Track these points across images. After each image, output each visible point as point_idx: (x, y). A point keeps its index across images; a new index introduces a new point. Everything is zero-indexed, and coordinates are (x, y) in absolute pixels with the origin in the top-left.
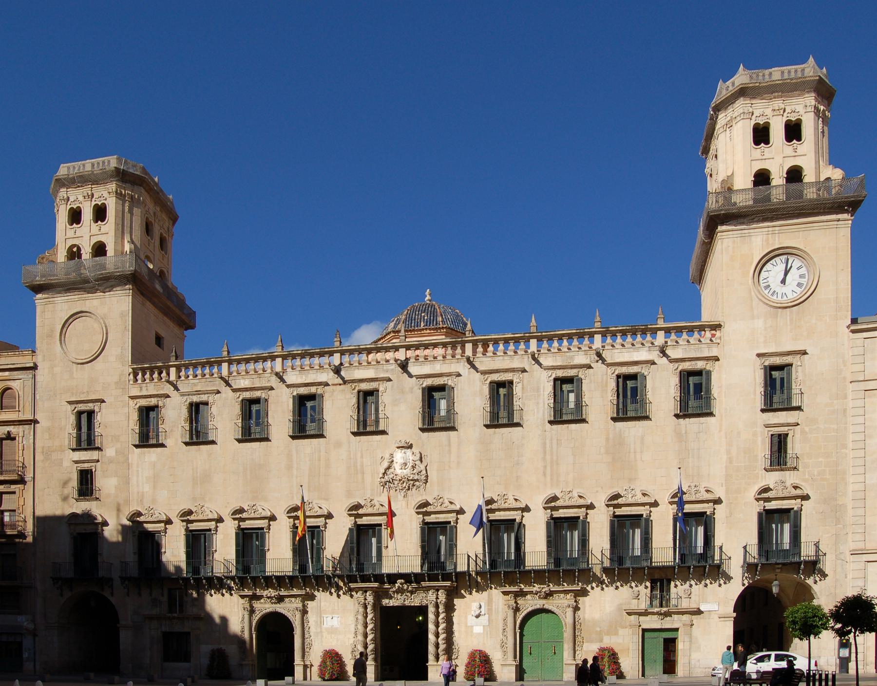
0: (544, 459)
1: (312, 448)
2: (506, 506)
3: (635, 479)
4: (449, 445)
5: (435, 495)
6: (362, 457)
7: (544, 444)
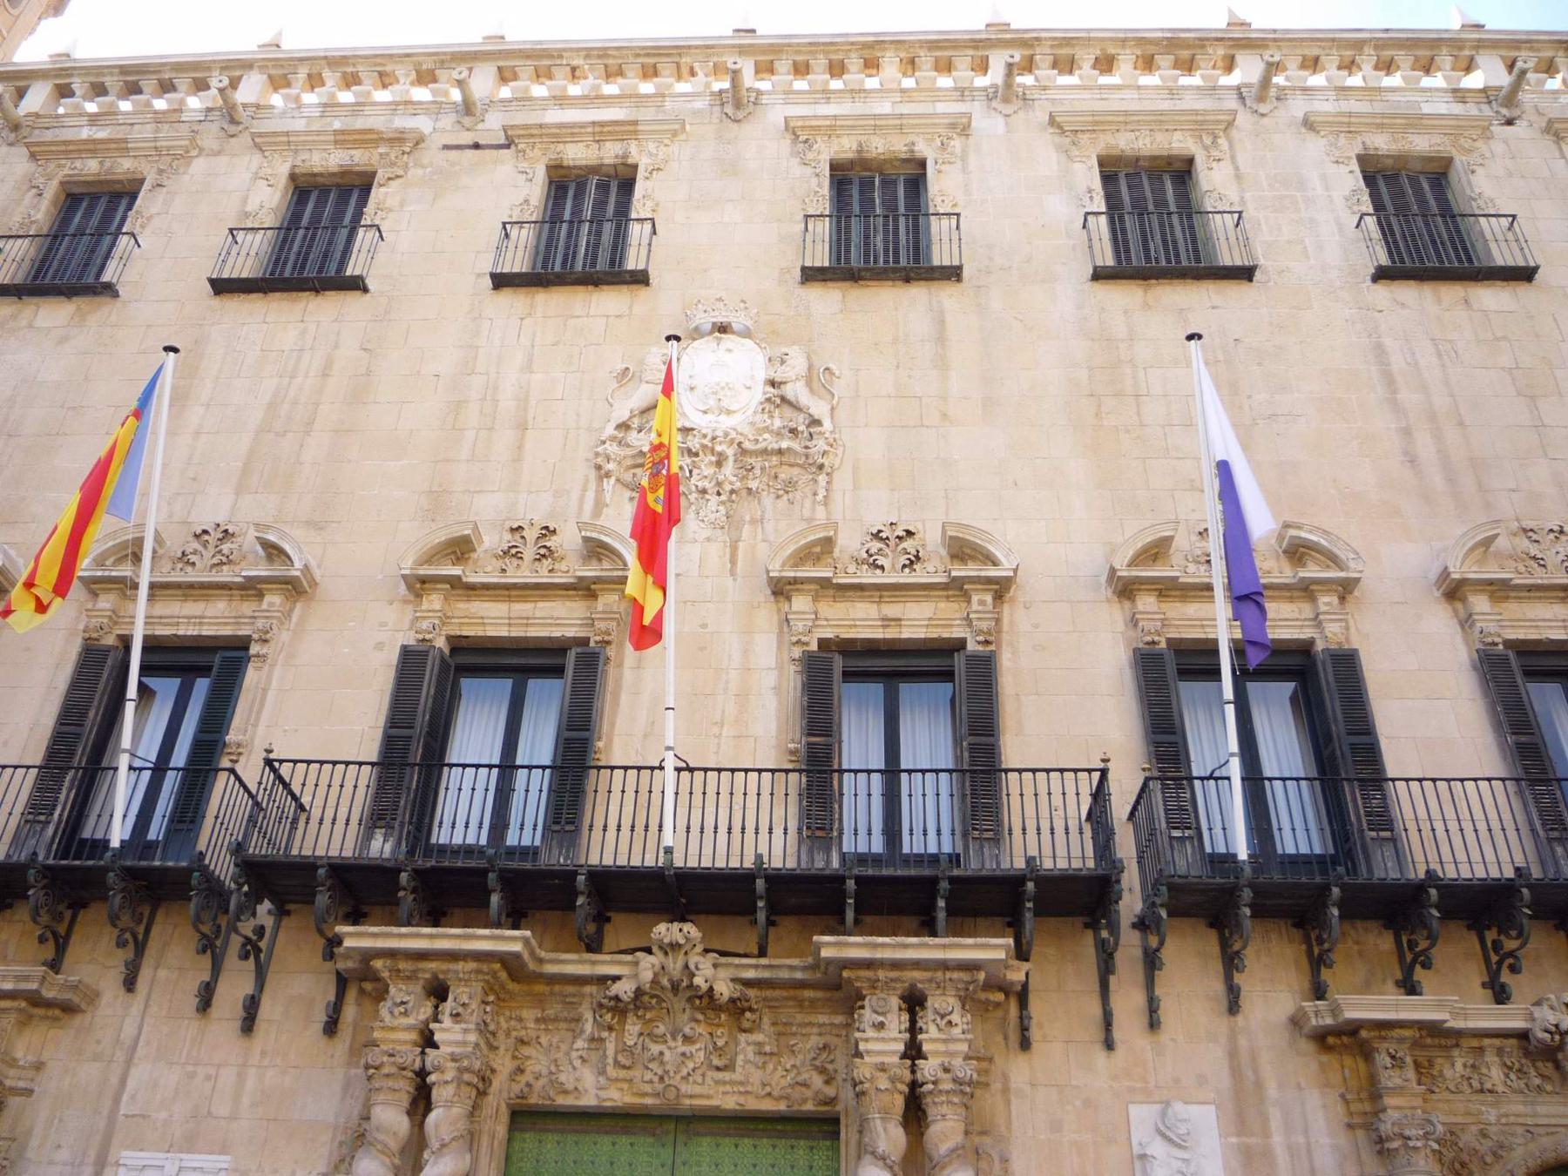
4: (941, 338)
6: (528, 367)
7: (1380, 351)
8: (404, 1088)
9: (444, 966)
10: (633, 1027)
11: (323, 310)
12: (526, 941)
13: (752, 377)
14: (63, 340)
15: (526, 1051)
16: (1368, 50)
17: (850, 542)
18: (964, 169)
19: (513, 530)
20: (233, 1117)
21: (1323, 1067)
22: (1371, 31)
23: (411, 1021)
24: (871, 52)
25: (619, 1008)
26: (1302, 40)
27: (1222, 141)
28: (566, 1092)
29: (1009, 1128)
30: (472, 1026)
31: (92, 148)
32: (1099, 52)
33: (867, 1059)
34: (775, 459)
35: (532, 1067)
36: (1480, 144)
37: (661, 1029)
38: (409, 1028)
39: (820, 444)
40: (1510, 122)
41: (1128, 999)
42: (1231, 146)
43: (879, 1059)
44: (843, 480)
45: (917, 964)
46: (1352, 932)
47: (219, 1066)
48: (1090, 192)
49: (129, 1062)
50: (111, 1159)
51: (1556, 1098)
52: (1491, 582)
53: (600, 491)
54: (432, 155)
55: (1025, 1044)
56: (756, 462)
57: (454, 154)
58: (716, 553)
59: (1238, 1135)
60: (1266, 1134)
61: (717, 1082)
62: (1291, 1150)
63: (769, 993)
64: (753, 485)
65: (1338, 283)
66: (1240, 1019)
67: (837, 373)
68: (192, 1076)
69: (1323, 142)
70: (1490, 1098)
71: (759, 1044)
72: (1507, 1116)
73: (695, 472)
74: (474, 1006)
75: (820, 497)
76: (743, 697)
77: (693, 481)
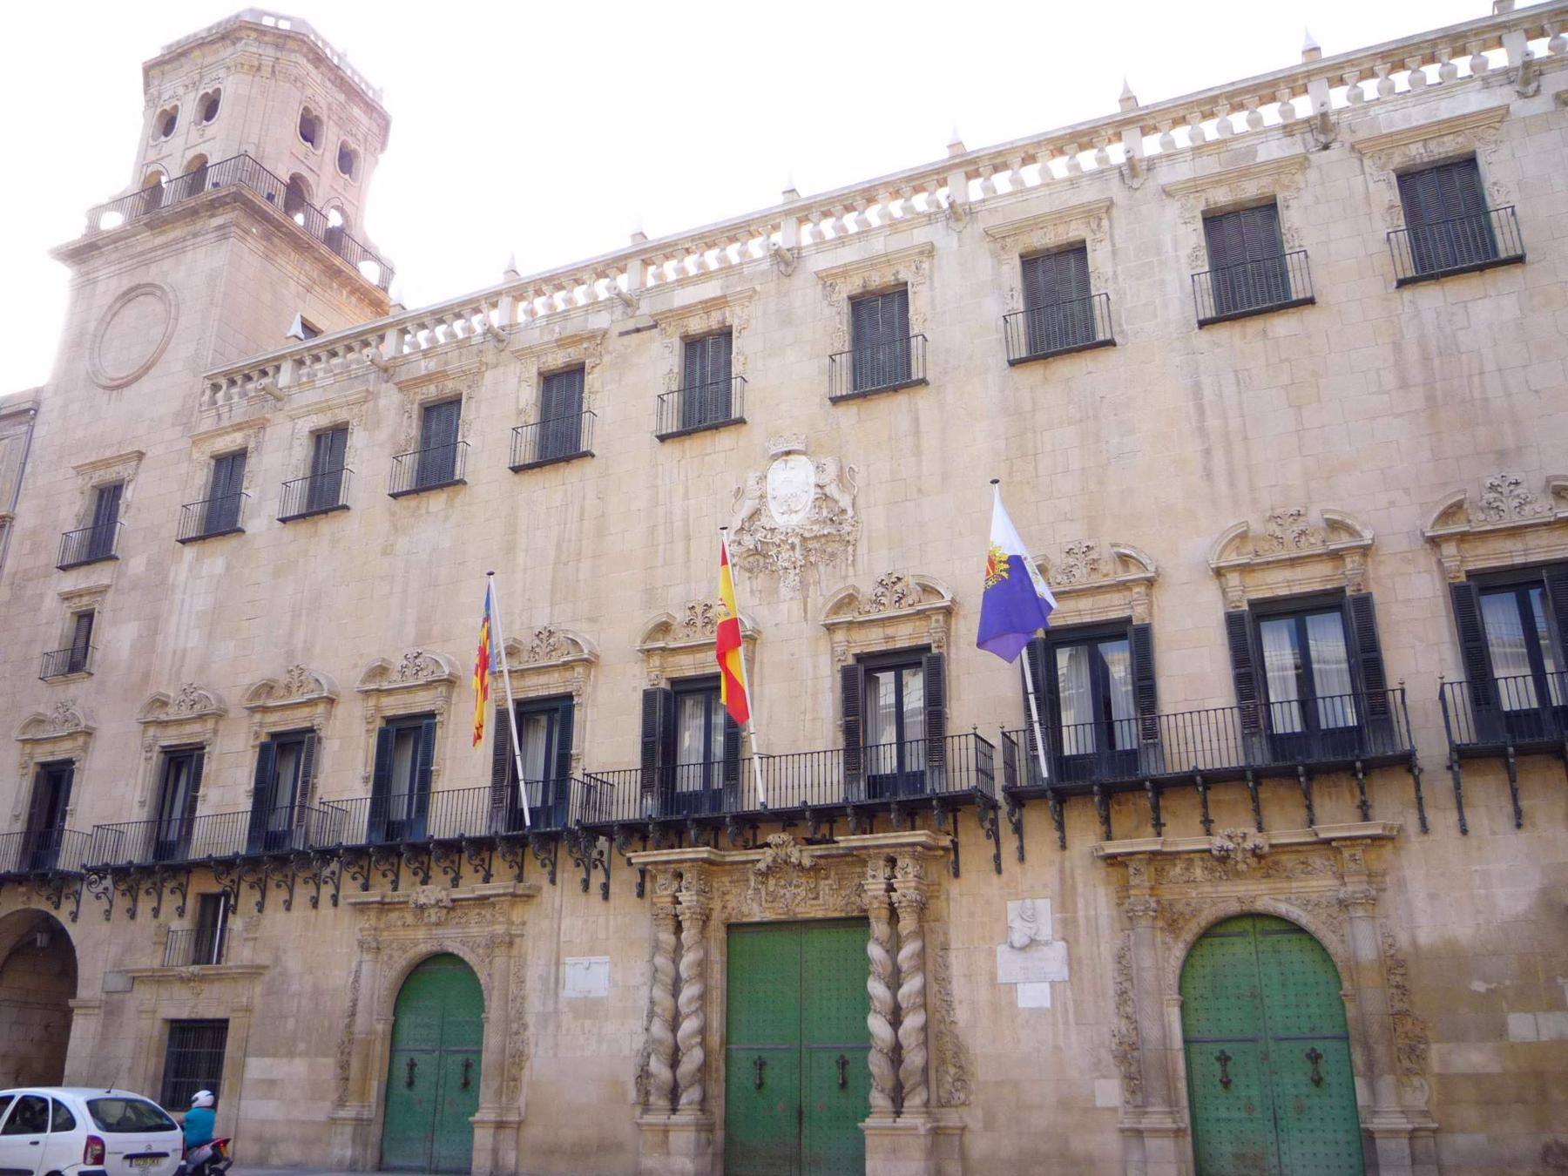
0: (1202, 430)
1: (566, 491)
2: (1097, 580)
3: (1519, 449)
4: (917, 433)
5: (881, 570)
6: (686, 496)
7: (1197, 389)
8: (670, 924)
9: (678, 865)
10: (772, 882)
11: (572, 474)
12: (709, 852)
13: (808, 484)
14: (446, 518)
15: (727, 897)
16: (1223, 101)
17: (867, 589)
18: (932, 288)
19: (690, 609)
20: (607, 939)
21: (1108, 874)
22: (1220, 87)
23: (669, 892)
24: (868, 194)
25: (765, 874)
26: (1168, 108)
27: (1105, 223)
28: (747, 916)
29: (949, 917)
30: (693, 892)
31: (430, 378)
32: (1023, 155)
33: (869, 893)
34: (823, 540)
35: (730, 905)
36: (1298, 177)
37: (783, 882)
38: (668, 896)
39: (846, 528)
40: (1326, 147)
41: (1009, 845)
42: (1111, 227)
43: (875, 893)
44: (862, 548)
45: (888, 846)
46: (1131, 797)
47: (598, 916)
48: (1012, 290)
49: (560, 918)
50: (562, 961)
51: (1229, 882)
52: (1239, 565)
54: (615, 343)
55: (957, 874)
56: (812, 545)
57: (627, 338)
58: (796, 607)
59: (1061, 912)
60: (1075, 911)
61: (812, 906)
62: (1087, 918)
63: (830, 860)
64: (813, 559)
65: (1175, 335)
66: (1067, 853)
67: (856, 470)
68: (587, 921)
69: (1178, 204)
70: (1193, 885)
71: (831, 885)
72: (1202, 893)
73: (780, 556)
74: (694, 882)
75: (849, 562)
76: (815, 695)
77: (779, 563)
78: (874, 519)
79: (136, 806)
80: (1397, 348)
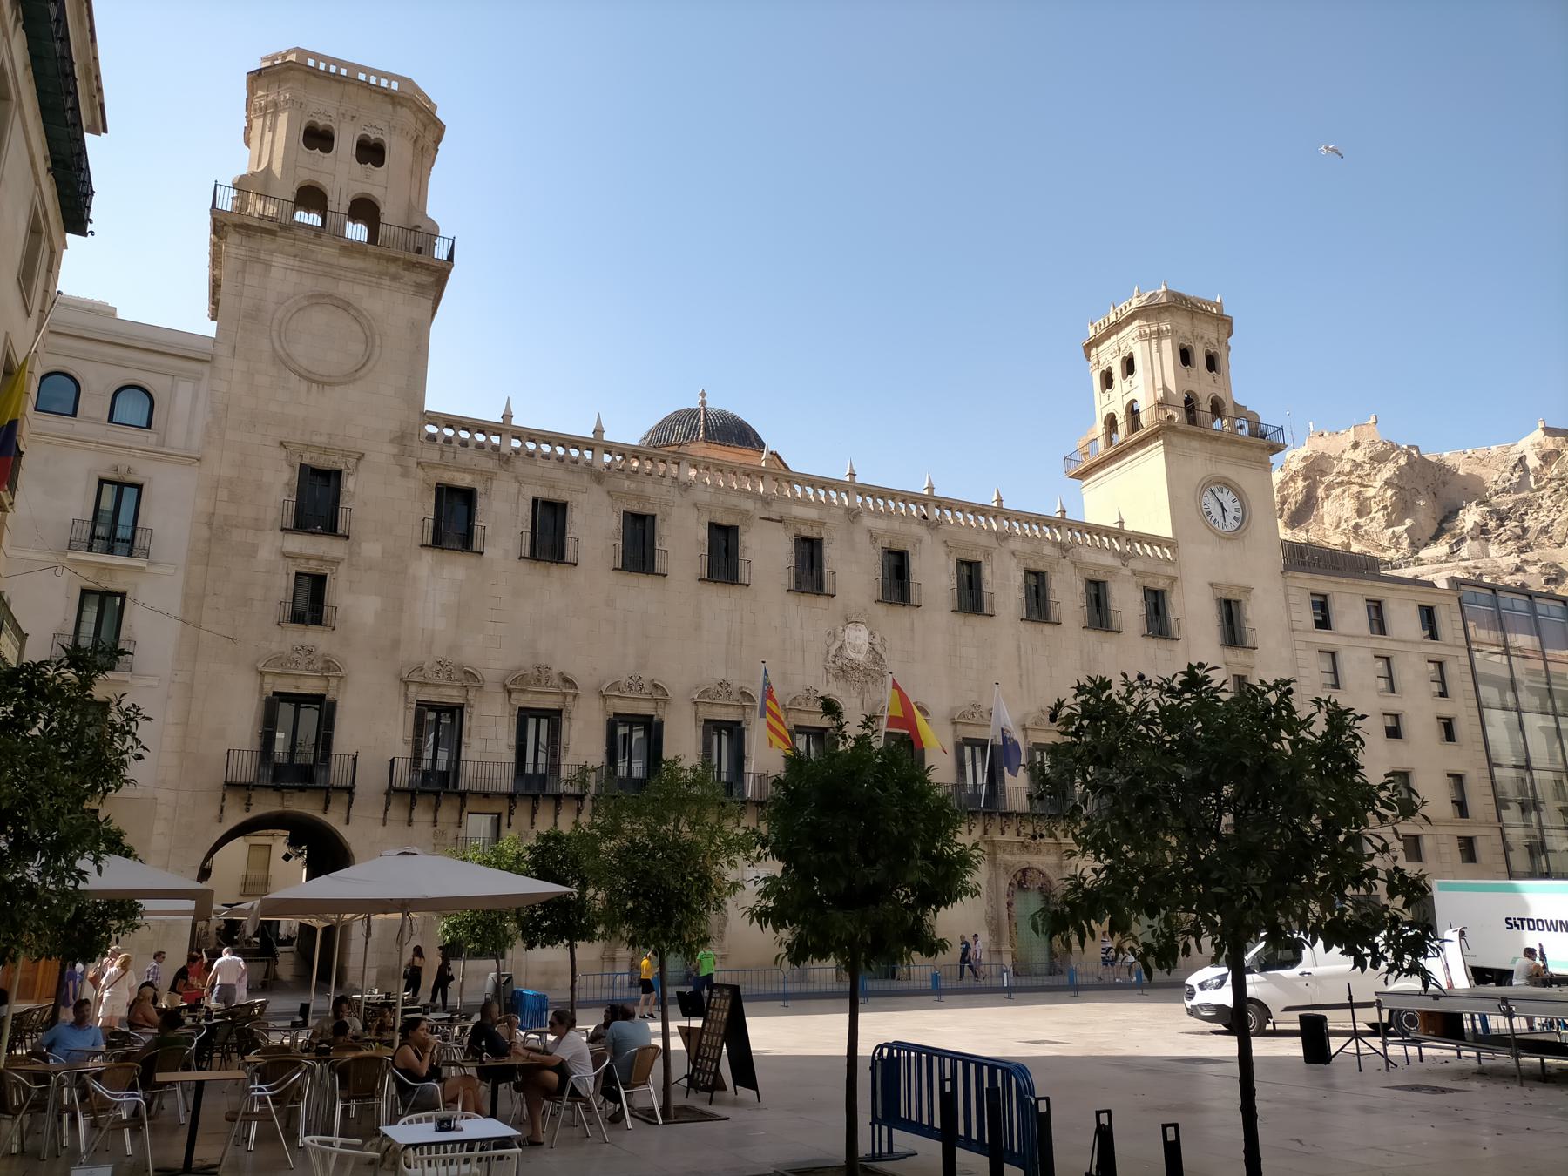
0: (1019, 665)
4: (912, 630)
6: (802, 628)
7: (1019, 647)
40: (1064, 558)
53: (827, 678)
58: (858, 702)
78: (893, 665)
79: (401, 743)
80: (1081, 651)
